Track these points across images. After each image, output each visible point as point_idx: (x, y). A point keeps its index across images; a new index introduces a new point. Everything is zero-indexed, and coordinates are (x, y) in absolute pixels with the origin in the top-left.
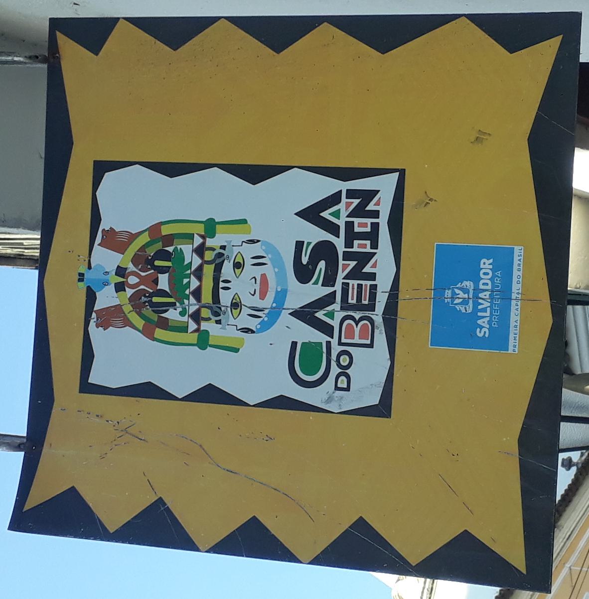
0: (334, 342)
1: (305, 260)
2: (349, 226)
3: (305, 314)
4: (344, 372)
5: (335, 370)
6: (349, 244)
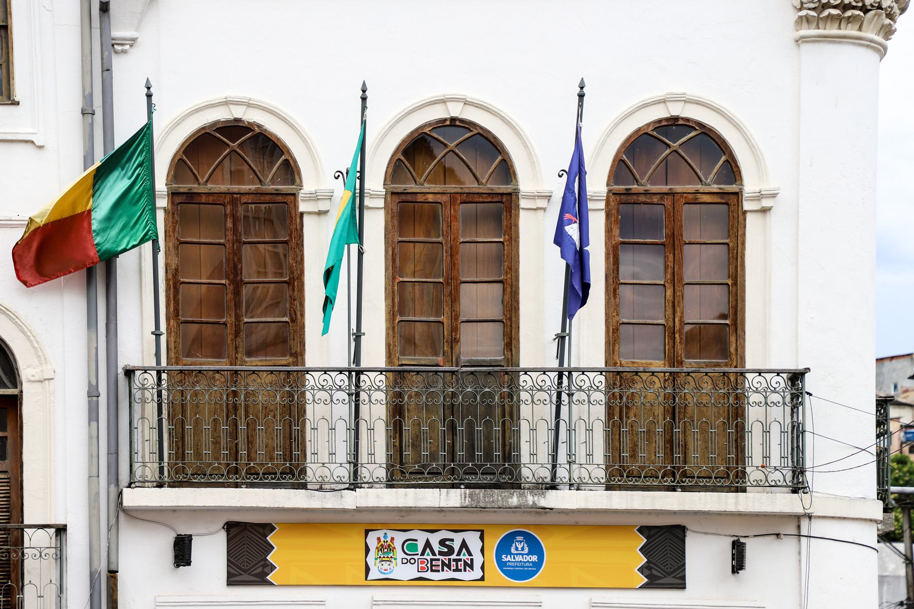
0: (419, 557)
1: (447, 543)
2: (460, 560)
3: (428, 545)
4: (408, 561)
5: (409, 557)
6: (454, 560)
